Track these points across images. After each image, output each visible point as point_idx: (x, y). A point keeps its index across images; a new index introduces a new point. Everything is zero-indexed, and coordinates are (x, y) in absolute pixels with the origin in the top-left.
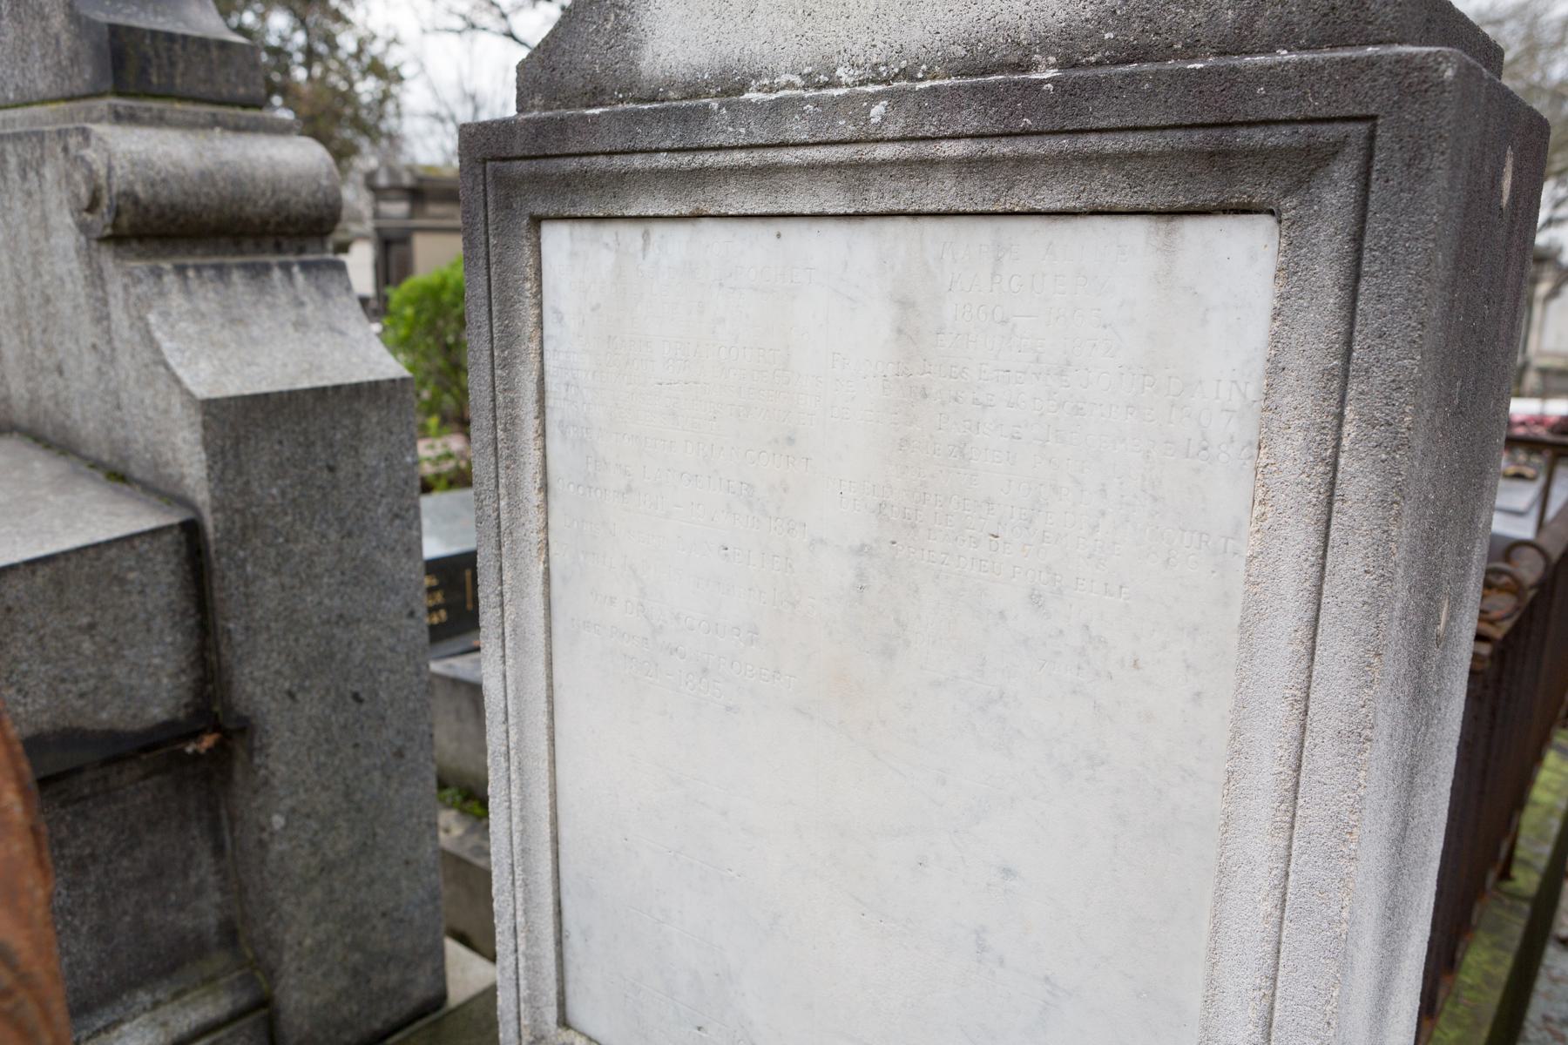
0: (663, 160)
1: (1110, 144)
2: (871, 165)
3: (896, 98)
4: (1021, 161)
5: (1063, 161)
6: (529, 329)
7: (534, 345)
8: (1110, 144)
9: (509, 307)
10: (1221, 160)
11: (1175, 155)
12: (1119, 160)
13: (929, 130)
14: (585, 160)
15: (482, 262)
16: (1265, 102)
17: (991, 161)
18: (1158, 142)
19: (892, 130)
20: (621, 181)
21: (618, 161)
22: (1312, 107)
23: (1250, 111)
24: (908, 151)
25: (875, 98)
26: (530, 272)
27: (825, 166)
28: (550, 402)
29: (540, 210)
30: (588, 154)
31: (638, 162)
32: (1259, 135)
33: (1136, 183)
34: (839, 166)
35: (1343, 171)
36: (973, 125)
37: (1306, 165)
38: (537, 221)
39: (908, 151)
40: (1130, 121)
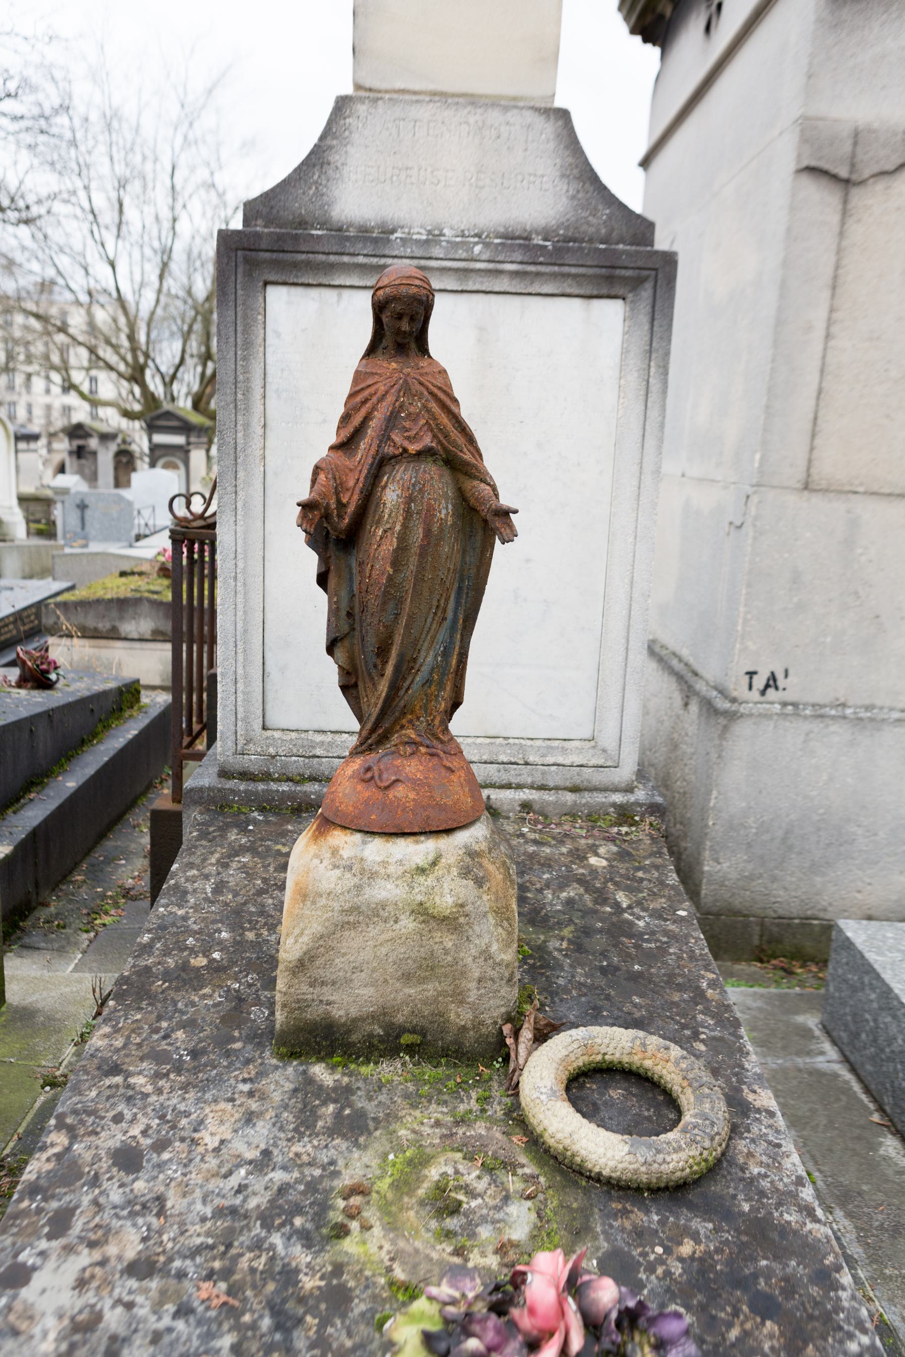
0: (361, 260)
1: (573, 270)
2: (472, 271)
3: (487, 245)
4: (538, 274)
5: (554, 276)
7: (262, 349)
8: (573, 270)
9: (247, 329)
10: (610, 279)
11: (595, 276)
12: (575, 276)
13: (500, 258)
14: (311, 256)
15: (232, 304)
16: (624, 260)
17: (525, 274)
18: (591, 271)
19: (485, 257)
20: (331, 268)
21: (332, 258)
22: (640, 264)
23: (619, 263)
24: (491, 266)
25: (476, 243)
26: (261, 310)
27: (450, 269)
29: (272, 277)
30: (313, 253)
31: (346, 259)
32: (623, 272)
33: (580, 285)
34: (457, 270)
35: (649, 285)
36: (519, 259)
37: (636, 283)
38: (266, 284)
39: (491, 266)
40: (580, 263)
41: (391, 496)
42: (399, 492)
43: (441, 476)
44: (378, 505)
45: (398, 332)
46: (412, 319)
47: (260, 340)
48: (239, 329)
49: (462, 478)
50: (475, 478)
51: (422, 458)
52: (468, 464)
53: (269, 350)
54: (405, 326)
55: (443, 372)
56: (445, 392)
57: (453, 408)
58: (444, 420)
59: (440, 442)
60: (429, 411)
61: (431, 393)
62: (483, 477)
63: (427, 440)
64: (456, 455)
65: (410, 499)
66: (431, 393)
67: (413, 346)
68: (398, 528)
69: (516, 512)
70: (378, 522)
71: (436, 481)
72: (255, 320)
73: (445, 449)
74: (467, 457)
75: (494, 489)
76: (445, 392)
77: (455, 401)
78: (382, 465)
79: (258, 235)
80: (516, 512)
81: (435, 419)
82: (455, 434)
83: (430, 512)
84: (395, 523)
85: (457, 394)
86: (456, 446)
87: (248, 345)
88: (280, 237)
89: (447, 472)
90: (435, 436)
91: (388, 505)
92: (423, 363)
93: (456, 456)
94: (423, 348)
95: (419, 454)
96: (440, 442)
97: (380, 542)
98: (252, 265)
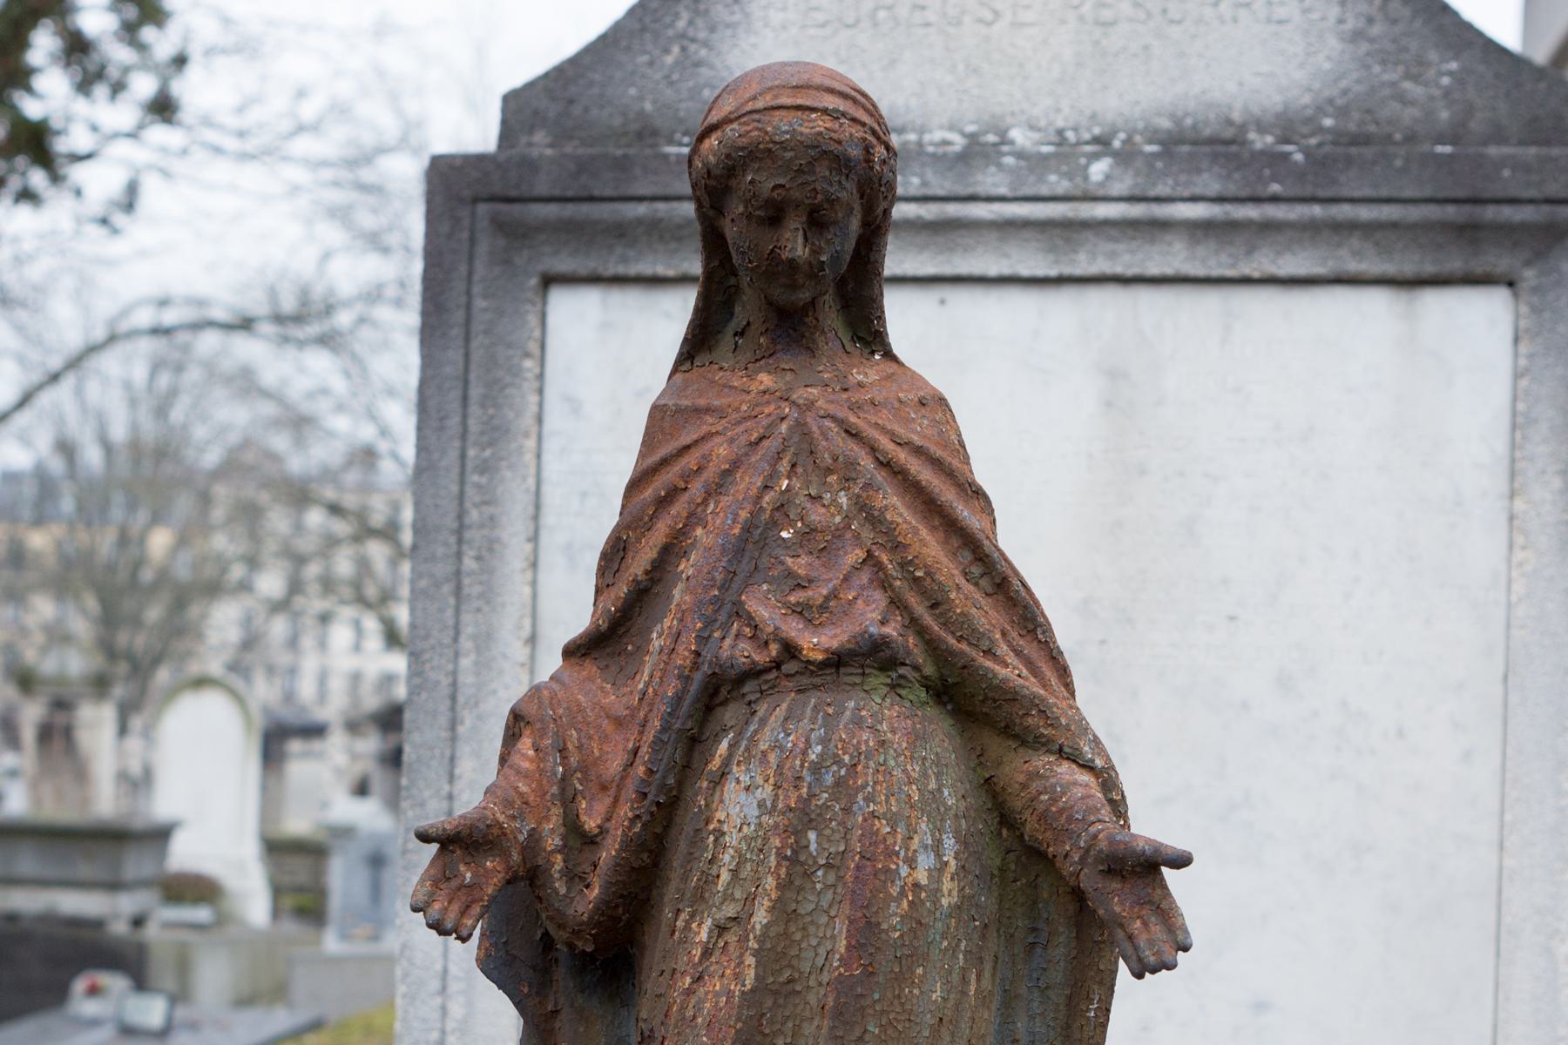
6: (528, 421)
7: (531, 443)
9: (496, 393)
26: (533, 347)
28: (549, 519)
29: (564, 265)
41: (740, 805)
42: (766, 792)
43: (916, 738)
44: (697, 839)
45: (778, 269)
46: (817, 222)
47: (528, 421)
48: (475, 392)
49: (995, 745)
50: (1039, 743)
51: (850, 676)
52: (1012, 696)
53: (551, 447)
54: (795, 245)
55: (935, 404)
56: (937, 464)
57: (965, 513)
58: (930, 547)
59: (914, 623)
60: (875, 520)
61: (886, 465)
62: (1071, 745)
63: (870, 616)
64: (967, 666)
65: (805, 817)
66: (886, 465)
67: (831, 317)
68: (761, 917)
69: (1181, 861)
70: (700, 897)
71: (902, 757)
72: (516, 372)
73: (932, 646)
74: (1010, 671)
75: (1108, 781)
76: (937, 464)
77: (977, 495)
78: (717, 694)
79: (529, 166)
80: (1181, 861)
81: (897, 547)
82: (987, 616)
83: (871, 868)
84: (750, 899)
85: (982, 475)
86: (971, 635)
87: (497, 433)
88: (583, 167)
89: (940, 735)
90: (897, 603)
91: (732, 839)
92: (867, 373)
93: (979, 679)
94: (869, 334)
95: (837, 662)
96: (914, 623)
97: (703, 971)
98: (516, 234)
